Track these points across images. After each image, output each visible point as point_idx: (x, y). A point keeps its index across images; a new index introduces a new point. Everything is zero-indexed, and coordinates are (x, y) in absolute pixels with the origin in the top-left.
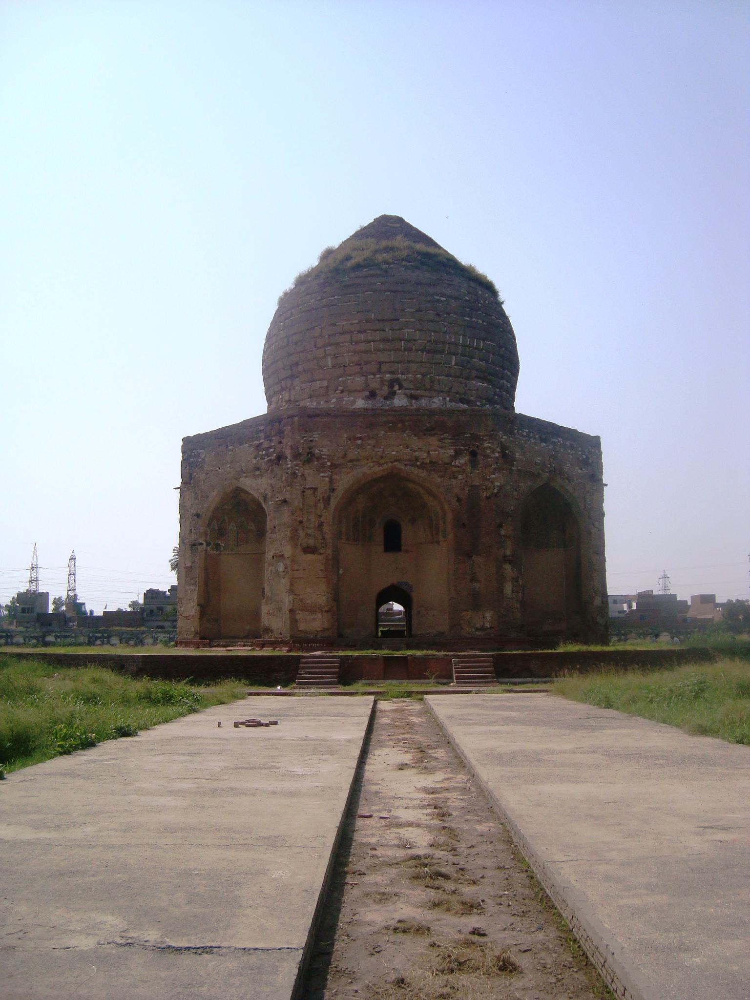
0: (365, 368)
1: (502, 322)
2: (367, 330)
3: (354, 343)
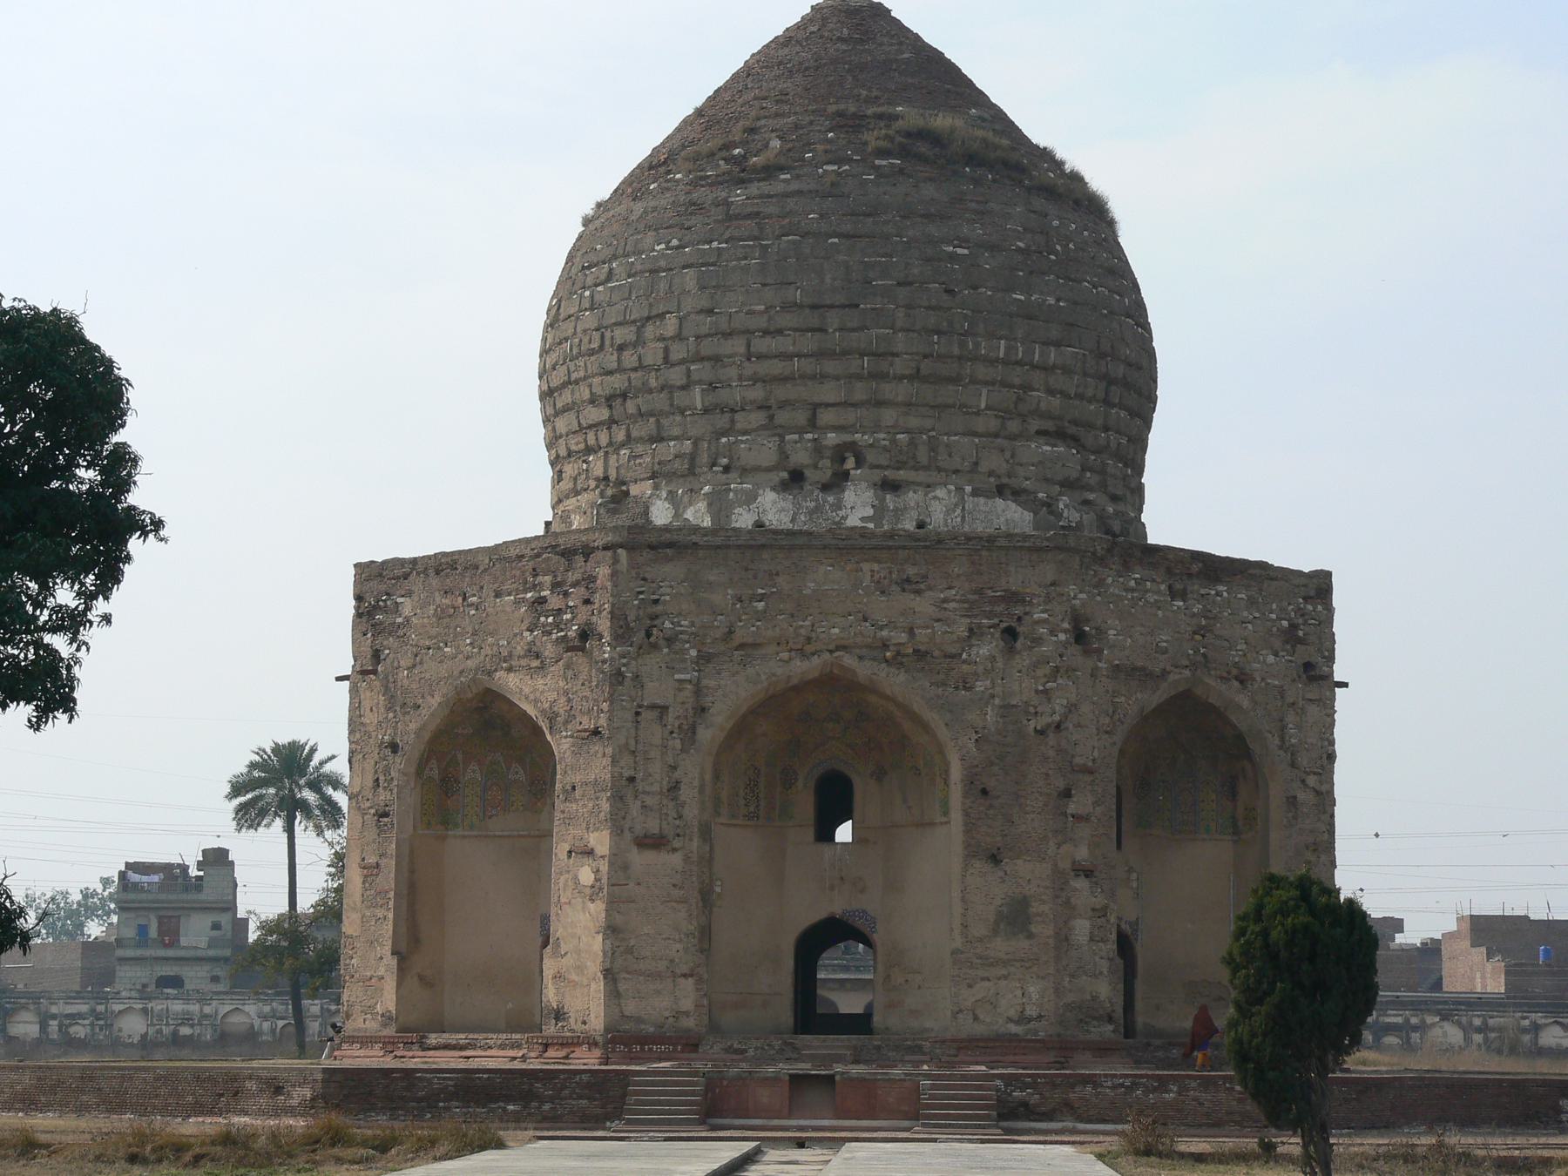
0: (782, 417)
1: (1107, 293)
2: (786, 330)
3: (754, 359)
